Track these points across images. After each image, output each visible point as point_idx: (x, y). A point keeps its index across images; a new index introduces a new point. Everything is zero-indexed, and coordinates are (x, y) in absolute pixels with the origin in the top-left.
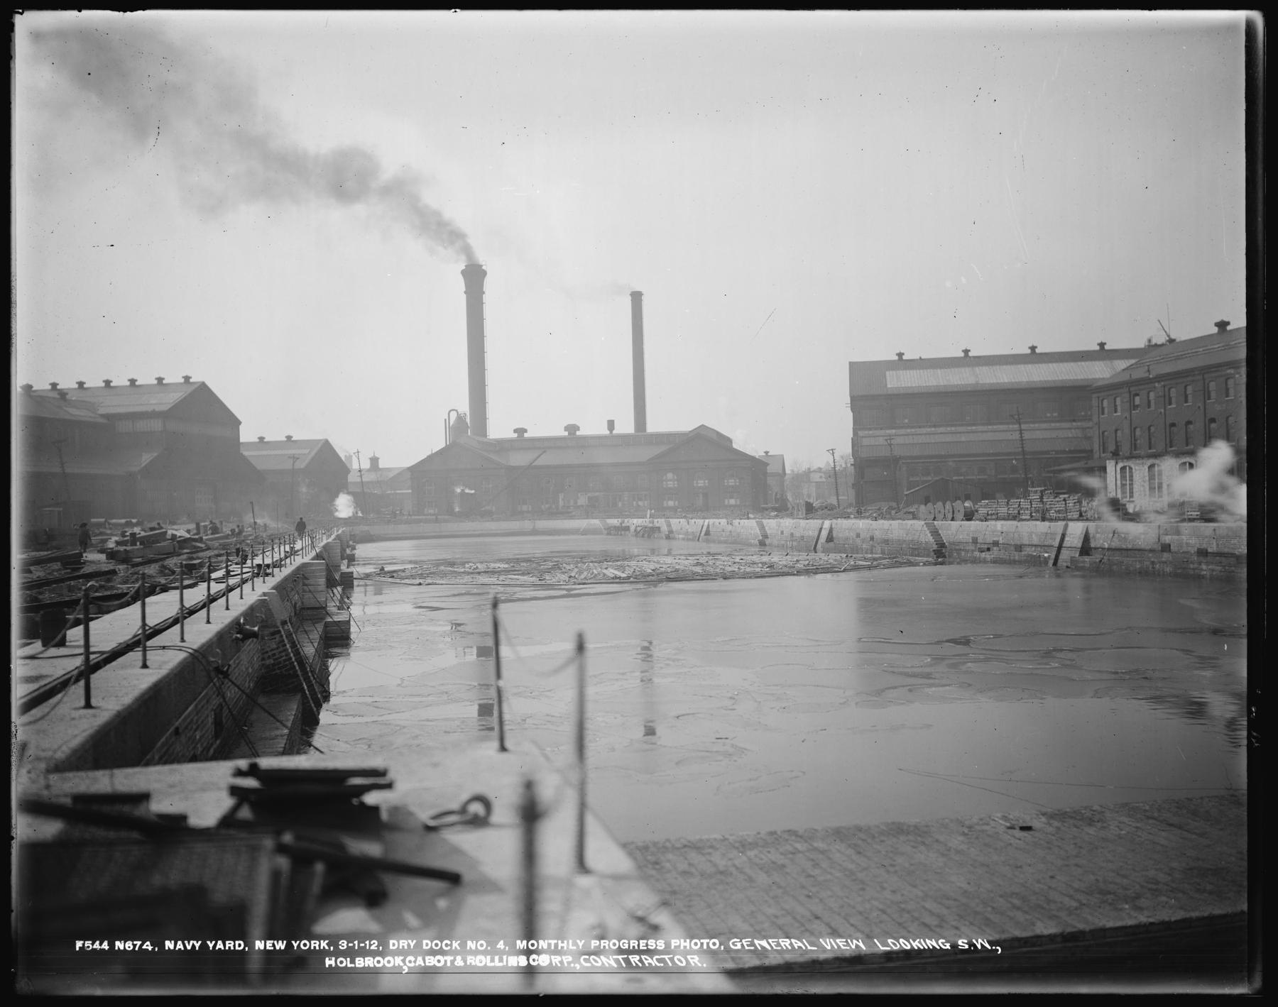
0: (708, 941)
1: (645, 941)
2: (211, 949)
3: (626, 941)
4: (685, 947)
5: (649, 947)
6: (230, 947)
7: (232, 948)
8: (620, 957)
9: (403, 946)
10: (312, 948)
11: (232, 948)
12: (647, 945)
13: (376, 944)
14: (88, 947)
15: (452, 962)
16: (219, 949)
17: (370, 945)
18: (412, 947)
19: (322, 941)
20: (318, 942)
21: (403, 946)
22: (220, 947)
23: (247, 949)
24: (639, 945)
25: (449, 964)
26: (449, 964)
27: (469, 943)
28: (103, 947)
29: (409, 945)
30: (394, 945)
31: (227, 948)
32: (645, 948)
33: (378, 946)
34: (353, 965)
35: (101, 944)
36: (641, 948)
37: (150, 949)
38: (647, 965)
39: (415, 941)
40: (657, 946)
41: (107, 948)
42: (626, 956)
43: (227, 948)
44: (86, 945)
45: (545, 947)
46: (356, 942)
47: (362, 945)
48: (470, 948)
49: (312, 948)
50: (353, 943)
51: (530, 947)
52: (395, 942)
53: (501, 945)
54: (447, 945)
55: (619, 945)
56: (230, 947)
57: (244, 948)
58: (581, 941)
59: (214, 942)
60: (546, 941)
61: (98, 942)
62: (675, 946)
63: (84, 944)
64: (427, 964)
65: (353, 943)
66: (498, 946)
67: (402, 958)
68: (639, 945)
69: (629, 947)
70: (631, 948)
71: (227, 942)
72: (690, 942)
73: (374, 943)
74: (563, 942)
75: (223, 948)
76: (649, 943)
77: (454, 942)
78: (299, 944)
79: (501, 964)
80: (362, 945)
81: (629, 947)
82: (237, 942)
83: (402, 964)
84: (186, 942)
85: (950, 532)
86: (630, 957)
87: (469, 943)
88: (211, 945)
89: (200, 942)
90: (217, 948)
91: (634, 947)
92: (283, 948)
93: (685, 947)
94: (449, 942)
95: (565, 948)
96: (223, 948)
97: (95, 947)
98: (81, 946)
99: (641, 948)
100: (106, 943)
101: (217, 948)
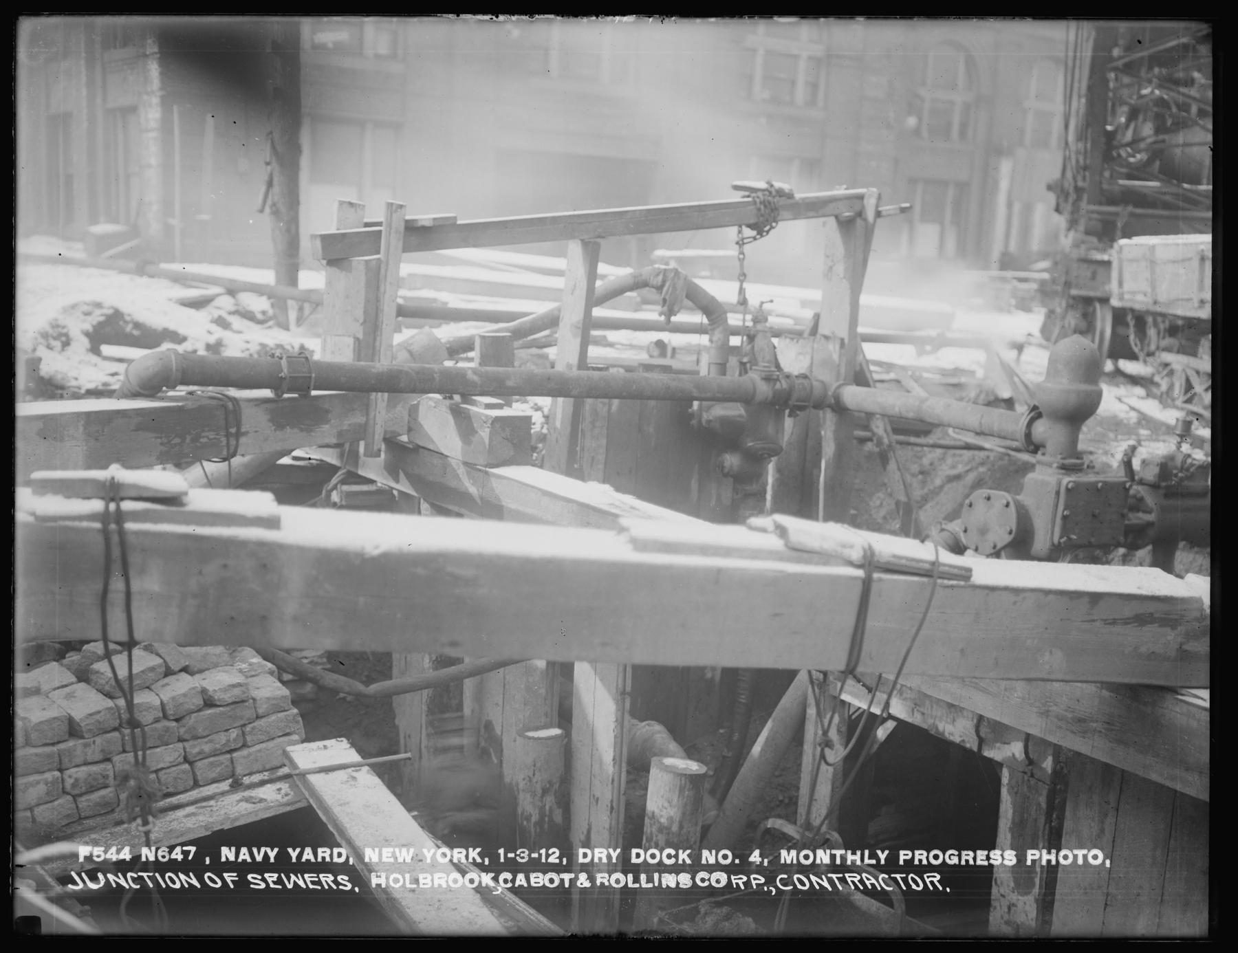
1: (986, 852)
2: (294, 860)
4: (1049, 861)
5: (992, 861)
6: (324, 858)
8: (834, 876)
9: (600, 859)
11: (328, 859)
12: (988, 858)
13: (557, 854)
17: (548, 856)
20: (328, 851)
21: (600, 859)
22: (308, 857)
24: (975, 859)
27: (705, 853)
29: (609, 857)
31: (320, 860)
33: (560, 858)
34: (637, 885)
36: (979, 862)
37: (179, 860)
38: (870, 887)
43: (320, 860)
48: (227, 858)
54: (669, 856)
55: (645, 854)
56: (324, 858)
58: (294, 850)
59: (298, 850)
62: (904, 860)
68: (975, 859)
69: (960, 860)
72: (1057, 854)
73: (554, 853)
78: (435, 854)
81: (960, 860)
85: (282, 374)
86: (847, 875)
87: (705, 853)
88: (294, 854)
89: (276, 850)
90: (303, 860)
91: (967, 861)
93: (1049, 861)
96: (313, 860)
101: (303, 860)
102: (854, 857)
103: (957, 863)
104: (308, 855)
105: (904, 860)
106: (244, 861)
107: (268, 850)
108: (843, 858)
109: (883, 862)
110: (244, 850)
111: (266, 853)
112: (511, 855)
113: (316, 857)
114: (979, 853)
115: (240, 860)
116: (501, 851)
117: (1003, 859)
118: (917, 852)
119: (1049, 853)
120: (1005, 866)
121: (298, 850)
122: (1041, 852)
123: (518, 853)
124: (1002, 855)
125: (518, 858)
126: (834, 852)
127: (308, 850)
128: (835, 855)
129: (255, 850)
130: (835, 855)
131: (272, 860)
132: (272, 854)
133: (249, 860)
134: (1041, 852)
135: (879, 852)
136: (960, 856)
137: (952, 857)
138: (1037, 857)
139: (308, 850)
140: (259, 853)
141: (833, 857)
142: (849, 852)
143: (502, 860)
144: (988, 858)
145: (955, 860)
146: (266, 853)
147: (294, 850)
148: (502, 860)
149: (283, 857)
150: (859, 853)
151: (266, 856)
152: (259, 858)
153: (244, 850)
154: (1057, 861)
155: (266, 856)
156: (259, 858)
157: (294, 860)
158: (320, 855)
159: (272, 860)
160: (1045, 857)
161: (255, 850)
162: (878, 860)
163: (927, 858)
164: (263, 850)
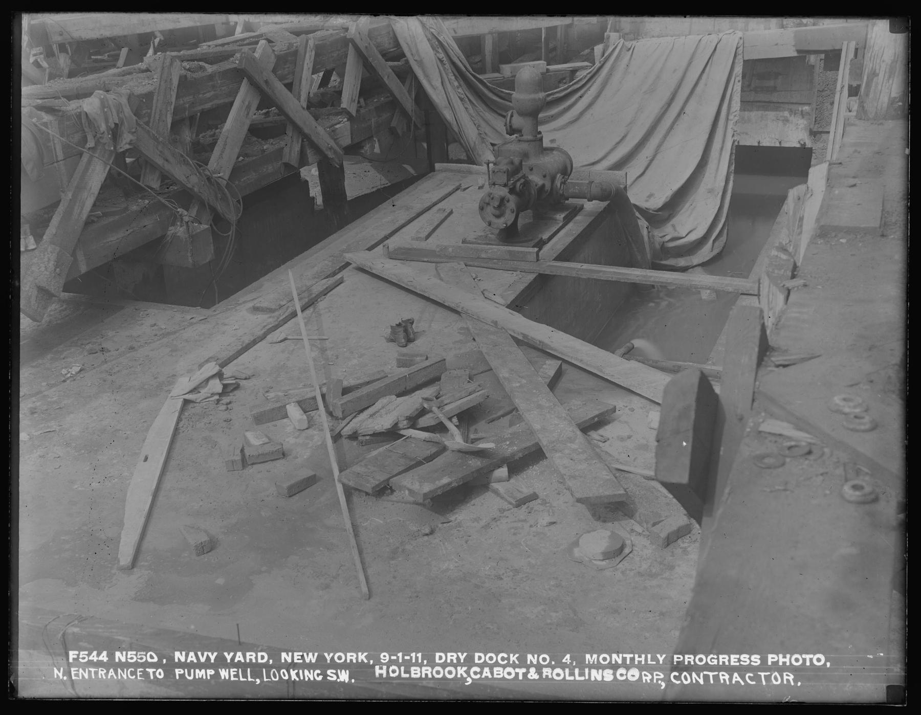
0: (811, 656)
2: (229, 661)
5: (742, 663)
6: (251, 660)
7: (254, 661)
10: (348, 661)
11: (254, 661)
12: (739, 660)
14: (84, 658)
15: (525, 675)
16: (191, 661)
18: (661, 662)
19: (360, 654)
24: (729, 661)
25: (521, 677)
26: (521, 677)
28: (101, 658)
30: (441, 658)
35: (98, 655)
36: (732, 664)
39: (465, 654)
41: (105, 659)
42: (716, 673)
44: (81, 656)
45: (620, 661)
46: (400, 655)
47: (407, 658)
49: (348, 661)
50: (410, 655)
51: (602, 661)
52: (443, 655)
53: (567, 658)
56: (251, 660)
59: (232, 654)
60: (621, 655)
61: (95, 653)
63: (78, 655)
64: (495, 676)
65: (410, 655)
66: (564, 661)
67: (465, 668)
68: (729, 661)
70: (721, 663)
71: (248, 654)
74: (640, 657)
75: (243, 661)
76: (742, 658)
77: (511, 655)
79: (582, 678)
80: (407, 658)
82: (260, 654)
83: (465, 675)
84: (199, 653)
88: (229, 657)
90: (236, 661)
94: (505, 656)
95: (643, 663)
96: (243, 661)
97: (91, 658)
98: (76, 657)
99: (732, 664)
100: (105, 653)
101: (236, 661)
104: (239, 657)
107: (210, 654)
108: (632, 659)
109: (661, 662)
110: (192, 654)
111: (208, 656)
113: (245, 657)
114: (732, 656)
115: (188, 661)
117: (751, 661)
118: (687, 656)
119: (784, 657)
121: (232, 654)
122: (778, 657)
124: (750, 659)
127: (239, 654)
129: (199, 653)
131: (212, 661)
132: (213, 658)
133: (195, 661)
134: (778, 657)
135: (658, 656)
136: (718, 659)
137: (713, 660)
139: (239, 654)
145: (715, 662)
146: (208, 656)
147: (229, 655)
150: (643, 656)
151: (208, 658)
152: (203, 660)
153: (192, 654)
155: (208, 658)
156: (203, 660)
157: (229, 661)
158: (248, 658)
159: (212, 661)
160: (781, 660)
162: (658, 661)
164: (206, 654)
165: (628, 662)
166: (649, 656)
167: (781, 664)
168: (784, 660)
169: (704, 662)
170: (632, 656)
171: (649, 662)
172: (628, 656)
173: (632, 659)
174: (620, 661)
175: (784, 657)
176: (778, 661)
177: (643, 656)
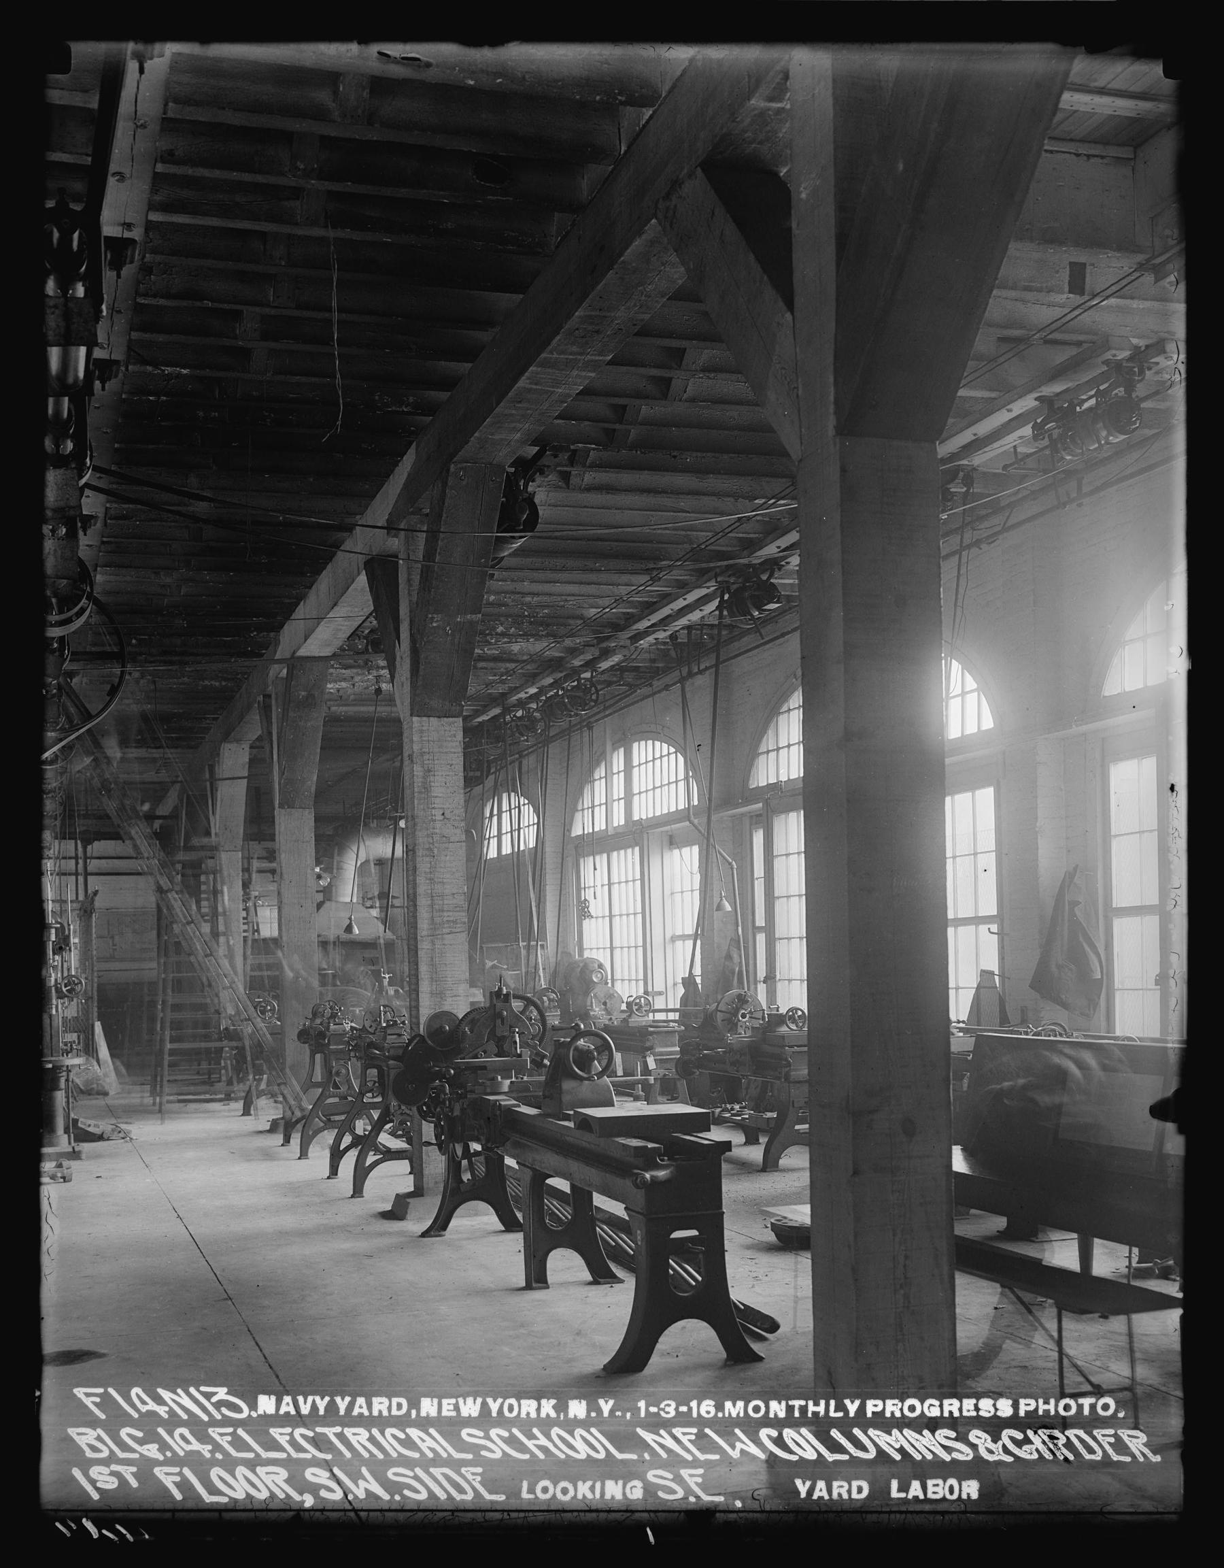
3: (937, 1403)
23: (414, 1413)
32: (974, 1414)
40: (996, 1409)
57: (409, 1412)
92: (475, 1414)
102: (816, 1409)
103: (939, 1414)
105: (873, 1413)
106: (287, 1413)
107: (318, 1399)
108: (803, 1410)
110: (287, 1399)
111: (314, 1401)
112: (653, 1409)
115: (282, 1412)
116: (642, 1404)
118: (889, 1402)
120: (999, 1417)
122: (1037, 1402)
123: (662, 1406)
125: (662, 1413)
126: (791, 1403)
128: (793, 1407)
129: (301, 1399)
130: (793, 1407)
131: (322, 1412)
132: (322, 1404)
134: (1037, 1402)
135: (847, 1402)
138: (879, 1409)
140: (305, 1403)
141: (790, 1409)
142: (811, 1403)
143: (643, 1414)
144: (977, 1409)
145: (935, 1412)
146: (314, 1401)
148: (643, 1414)
149: (332, 1407)
150: (823, 1402)
152: (305, 1410)
153: (287, 1399)
154: (1056, 1411)
155: (314, 1407)
156: (305, 1410)
159: (322, 1412)
160: (1042, 1408)
161: (301, 1399)
163: (901, 1410)
164: (310, 1399)
165: (797, 1414)
166: (832, 1403)
167: (1041, 1412)
168: (1046, 1407)
169: (918, 1412)
170: (803, 1403)
171: (832, 1414)
172: (797, 1403)
173: (803, 1410)
174: (782, 1415)
175: (1047, 1402)
176: (1037, 1406)
177: (823, 1402)
